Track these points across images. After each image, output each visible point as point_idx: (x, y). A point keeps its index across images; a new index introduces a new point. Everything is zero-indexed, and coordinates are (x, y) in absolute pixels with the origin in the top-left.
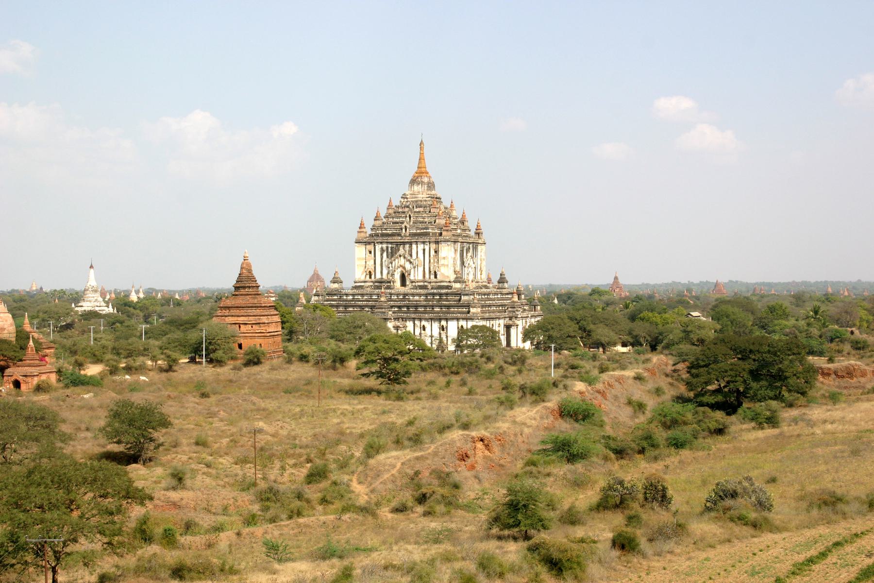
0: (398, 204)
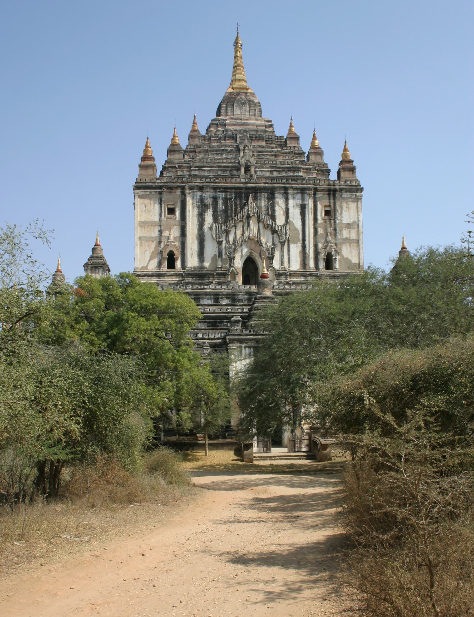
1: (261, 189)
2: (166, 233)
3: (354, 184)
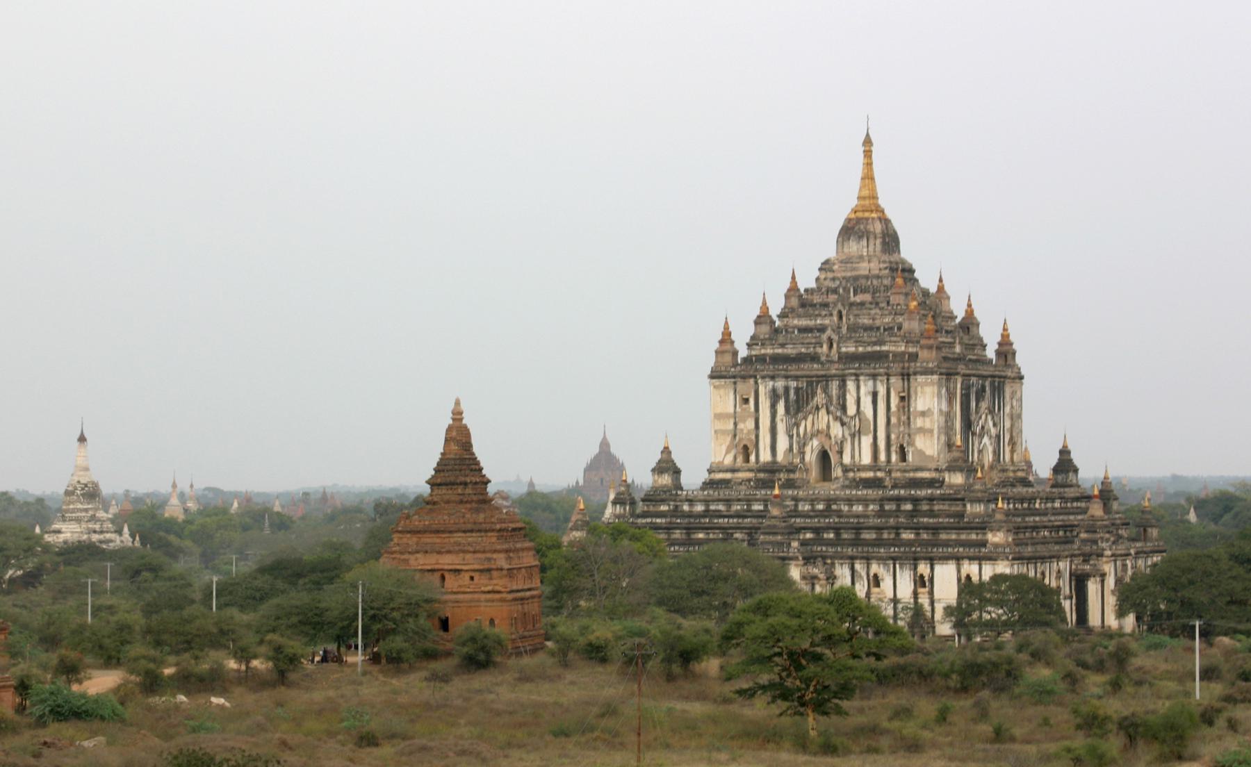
0: (813, 285)
2: (741, 426)
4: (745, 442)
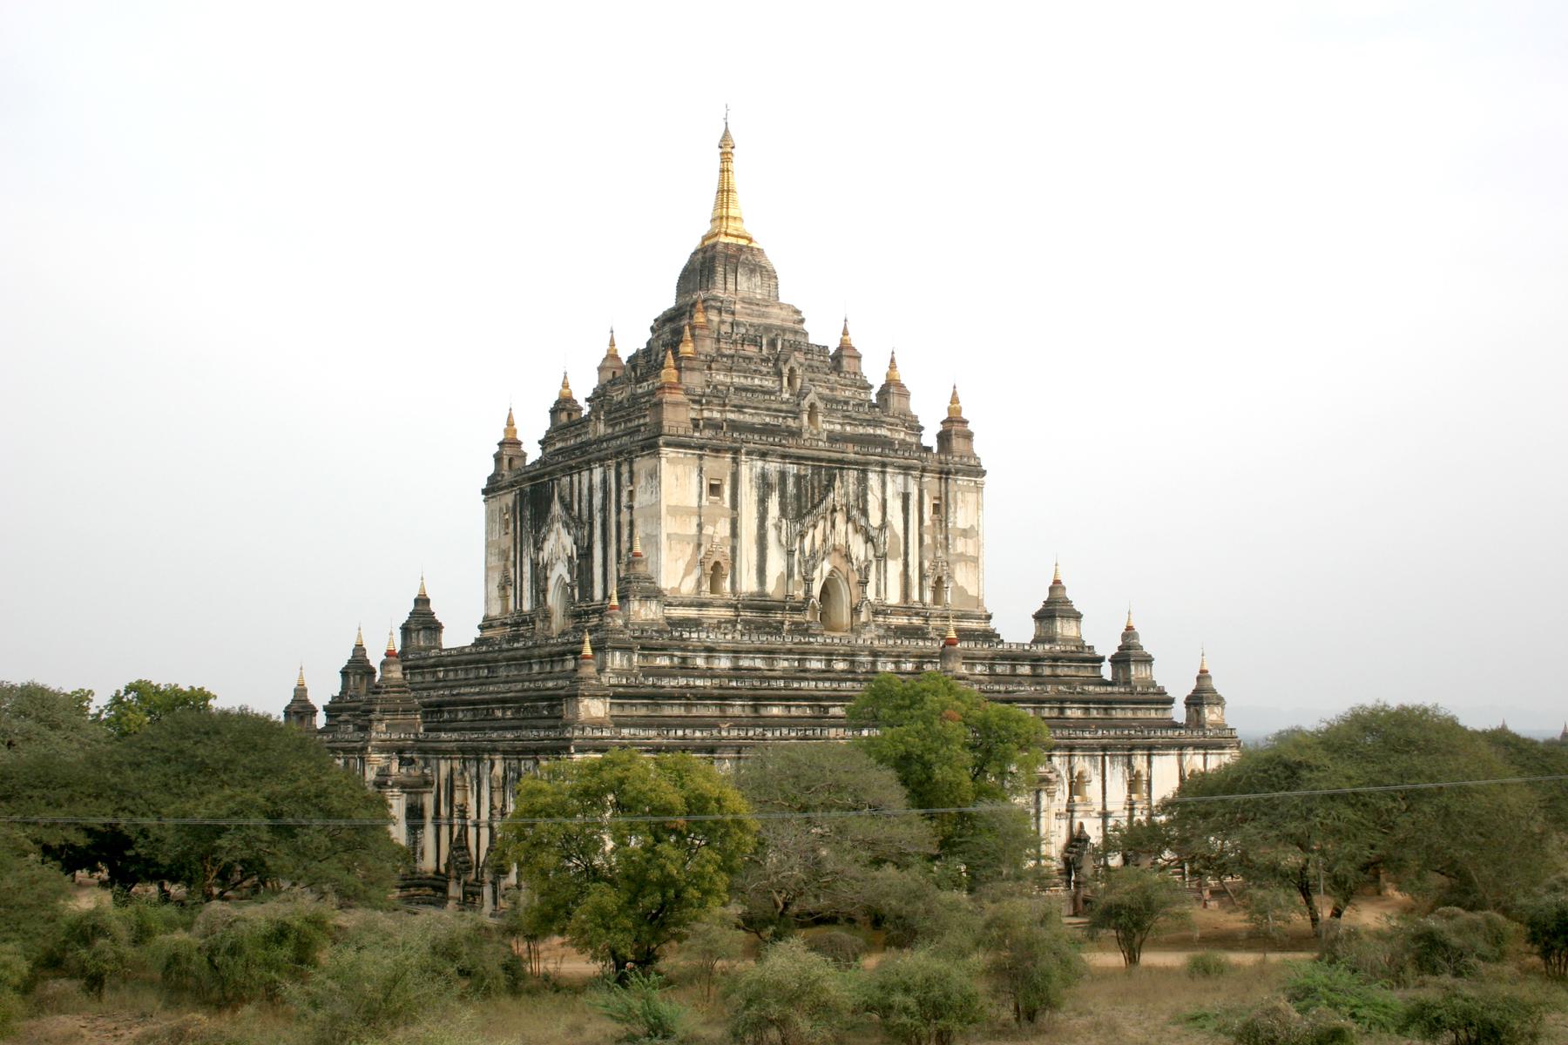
1: (849, 463)
2: (708, 530)
3: (973, 462)
4: (716, 558)
